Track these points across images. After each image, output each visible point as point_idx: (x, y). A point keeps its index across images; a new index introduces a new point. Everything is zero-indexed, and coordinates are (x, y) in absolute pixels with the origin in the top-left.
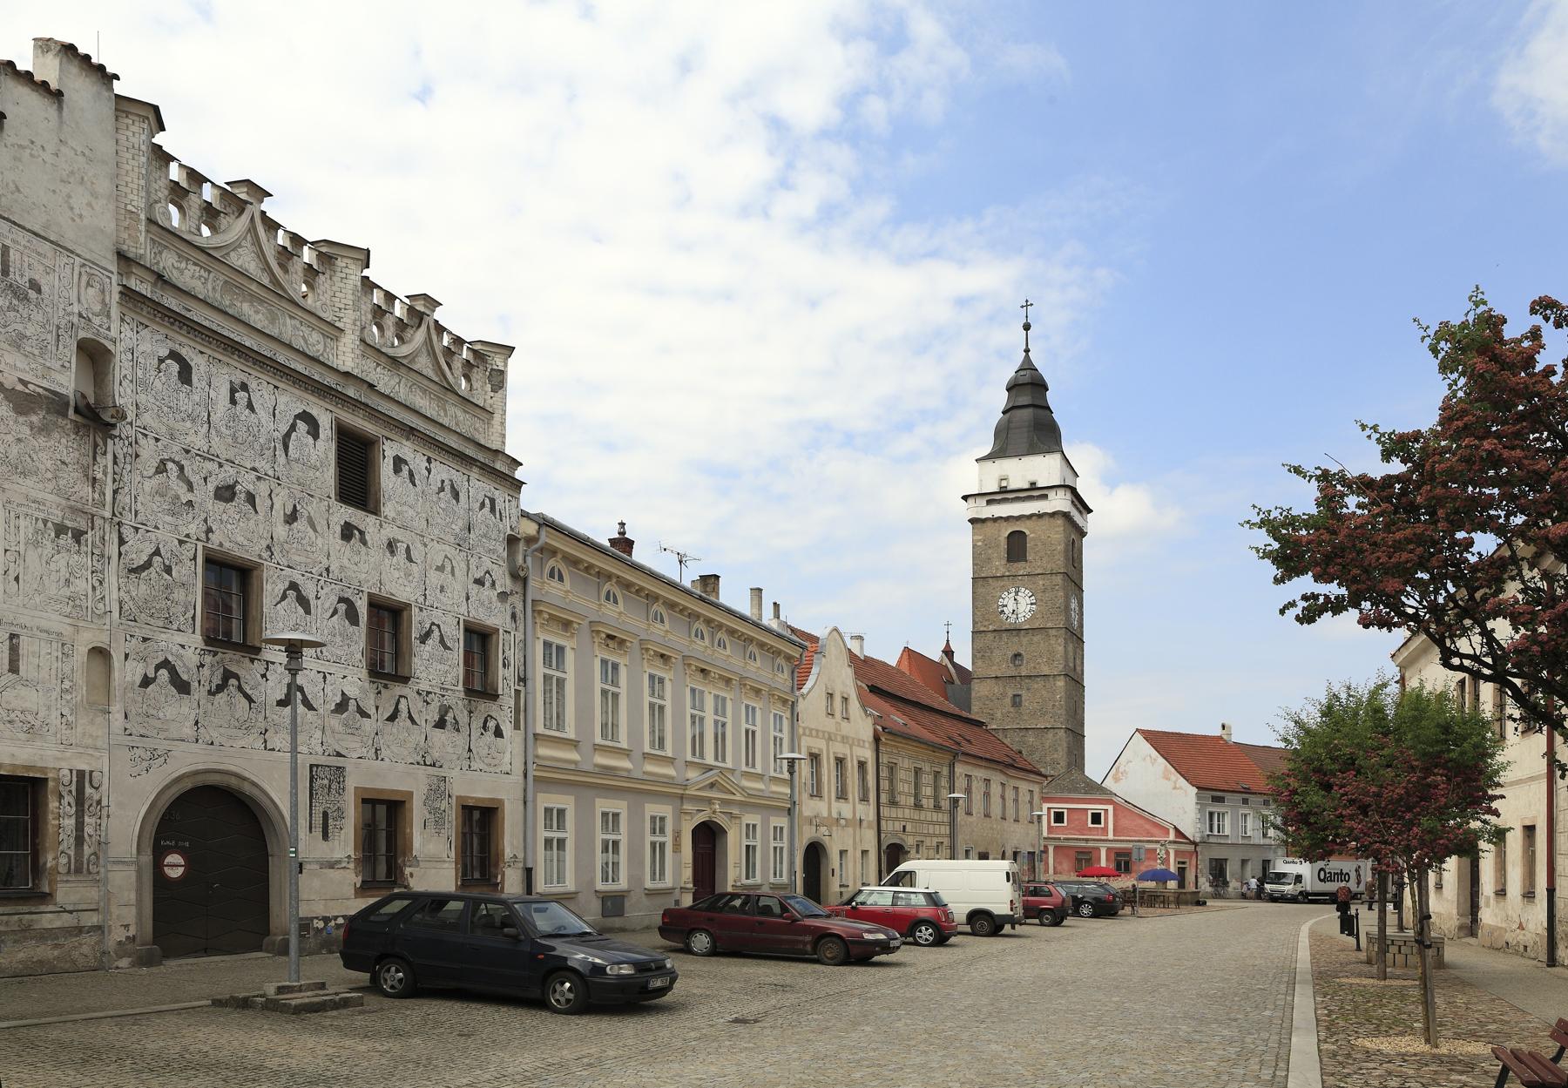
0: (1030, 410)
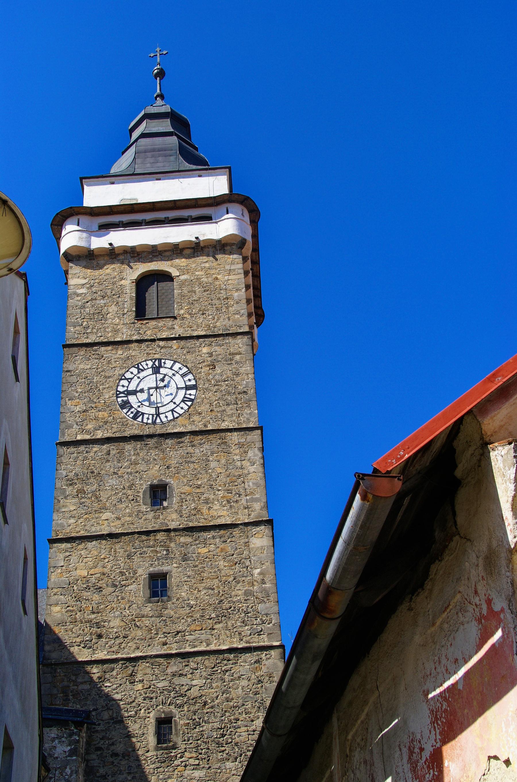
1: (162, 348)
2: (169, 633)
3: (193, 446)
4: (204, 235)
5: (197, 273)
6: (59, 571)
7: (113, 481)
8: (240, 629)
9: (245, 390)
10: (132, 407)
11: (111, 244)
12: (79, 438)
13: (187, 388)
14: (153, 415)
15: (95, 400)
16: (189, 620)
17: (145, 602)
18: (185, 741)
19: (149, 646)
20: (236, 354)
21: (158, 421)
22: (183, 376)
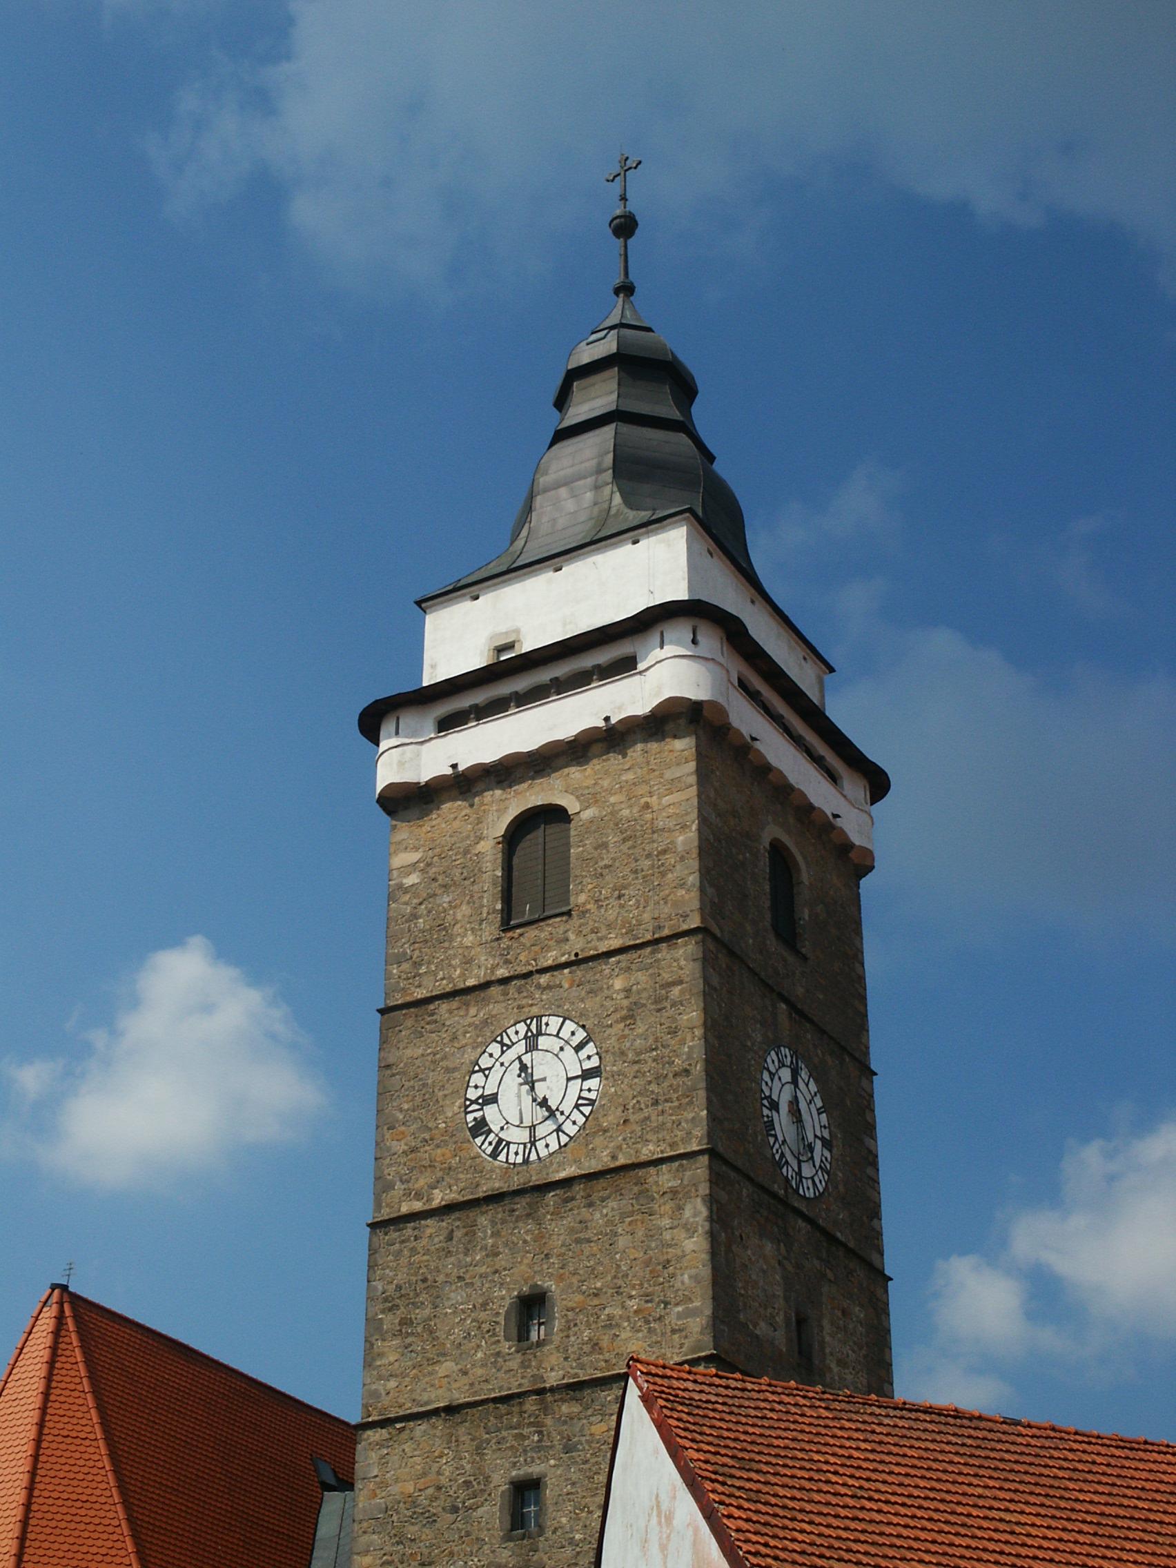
0: (608, 432)
1: (545, 989)
3: (590, 1205)
4: (620, 708)
5: (612, 799)
6: (372, 1486)
7: (457, 1296)
9: (685, 1066)
10: (490, 1131)
12: (405, 1209)
13: (587, 1075)
14: (525, 1144)
17: (502, 1538)
20: (674, 984)
21: (533, 1157)
22: (579, 1048)
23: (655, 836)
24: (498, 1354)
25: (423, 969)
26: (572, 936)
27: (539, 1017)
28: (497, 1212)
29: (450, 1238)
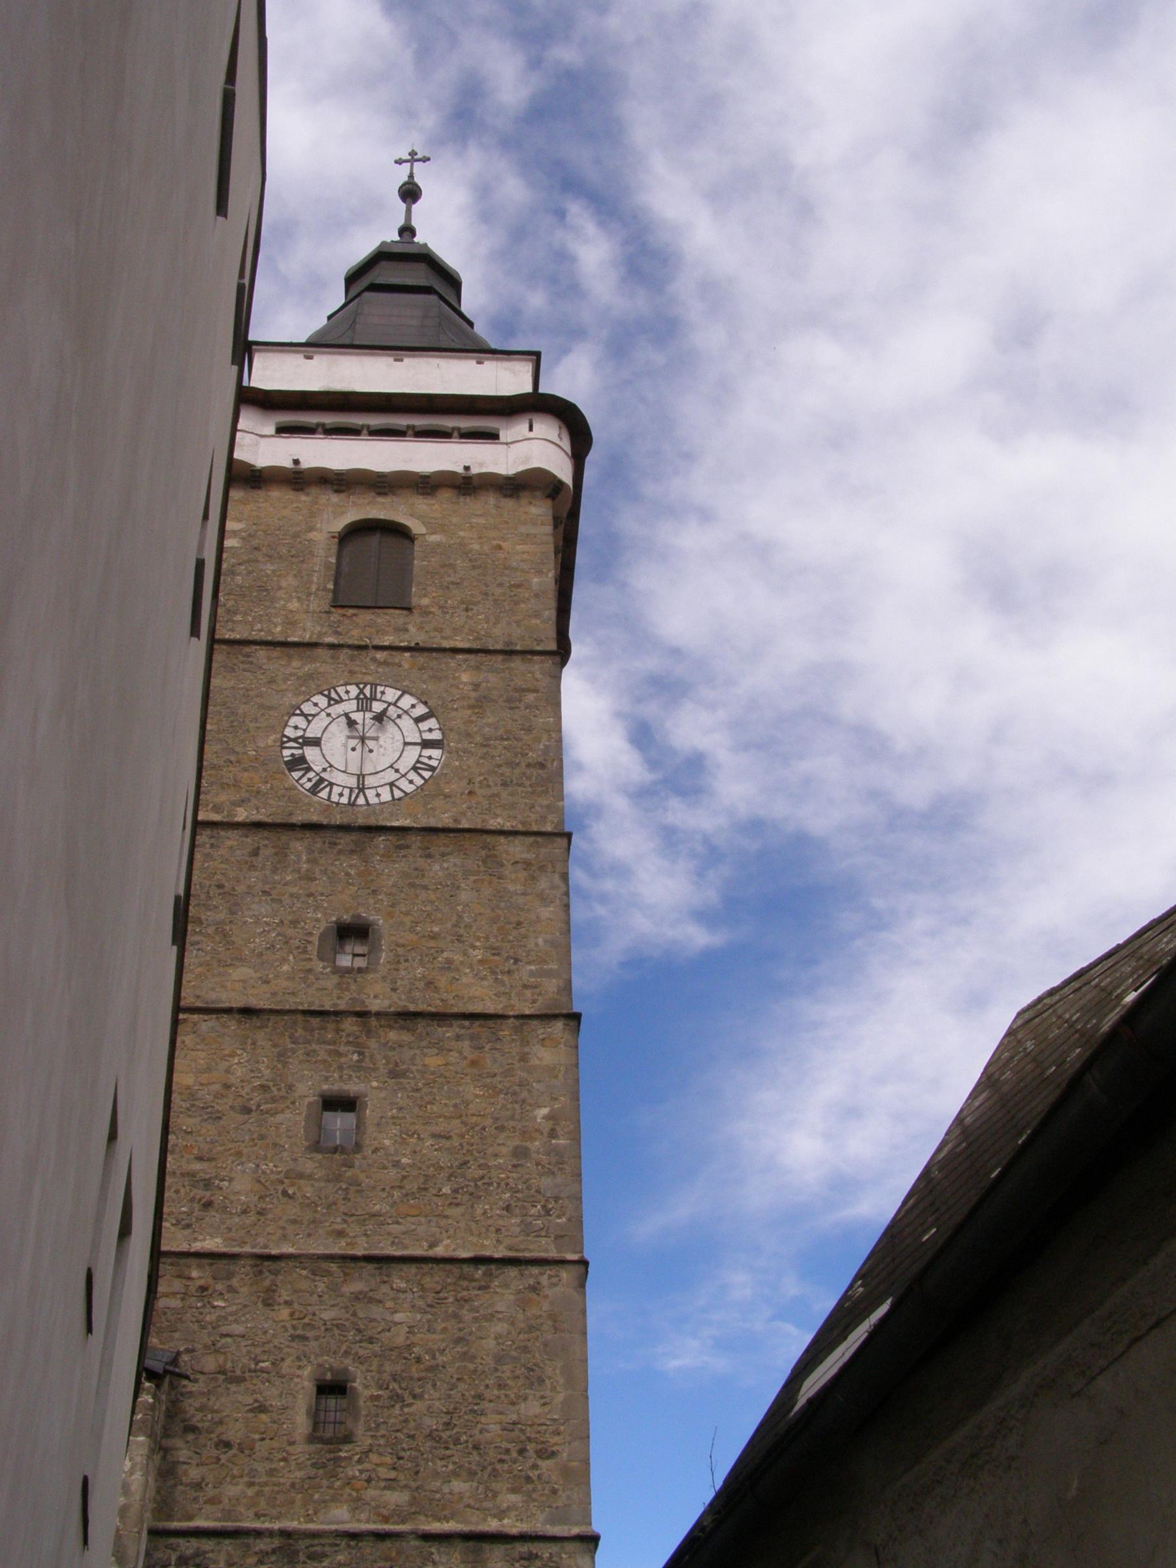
2: (353, 1215)
3: (429, 856)
4: (481, 465)
5: (462, 534)
8: (501, 1222)
9: (541, 759)
10: (309, 769)
11: (296, 462)
13: (426, 744)
14: (351, 789)
15: (237, 749)
16: (397, 1194)
18: (370, 1430)
19: (309, 1235)
20: (528, 690)
22: (418, 720)
23: (507, 572)
24: (310, 971)
25: (239, 618)
26: (412, 628)
27: (374, 685)
28: (318, 841)
29: (255, 853)
